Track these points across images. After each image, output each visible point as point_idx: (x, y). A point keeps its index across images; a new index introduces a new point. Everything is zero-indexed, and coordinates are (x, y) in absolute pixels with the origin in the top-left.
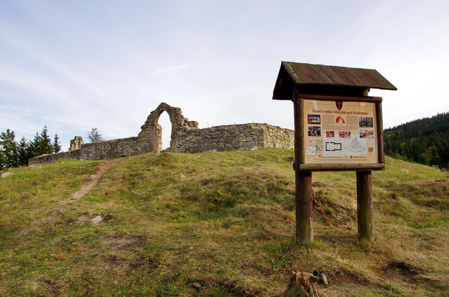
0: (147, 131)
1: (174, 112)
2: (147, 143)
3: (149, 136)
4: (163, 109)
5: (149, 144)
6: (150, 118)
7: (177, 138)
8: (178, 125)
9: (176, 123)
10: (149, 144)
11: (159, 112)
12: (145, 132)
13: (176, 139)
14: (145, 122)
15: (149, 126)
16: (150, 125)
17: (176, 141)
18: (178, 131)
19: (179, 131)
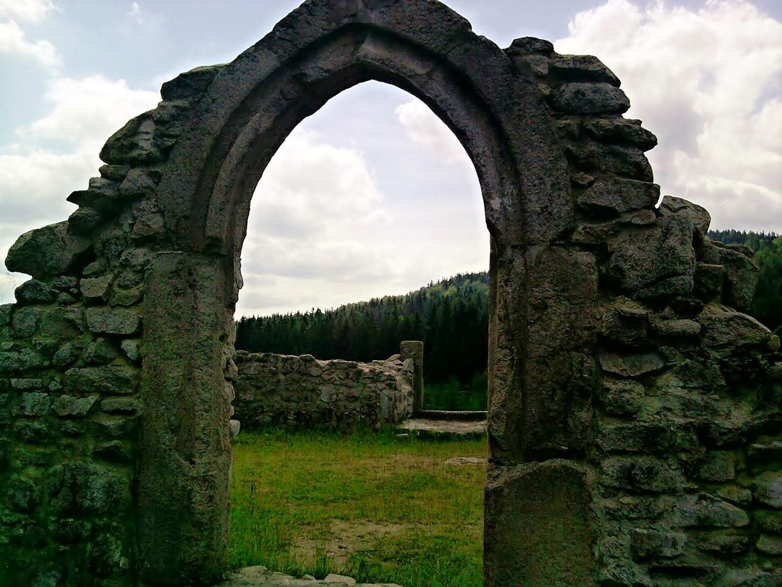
0: (96, 302)
1: (561, 111)
2: (100, 468)
3: (128, 372)
4: (370, 50)
5: (119, 475)
6: (146, 144)
7: (611, 465)
8: (632, 278)
9: (586, 258)
10: (135, 486)
11: (293, 91)
12: (74, 312)
13: (591, 475)
14: (74, 197)
15: (140, 255)
16: (140, 242)
17: (601, 503)
18: (609, 364)
19: (651, 363)
